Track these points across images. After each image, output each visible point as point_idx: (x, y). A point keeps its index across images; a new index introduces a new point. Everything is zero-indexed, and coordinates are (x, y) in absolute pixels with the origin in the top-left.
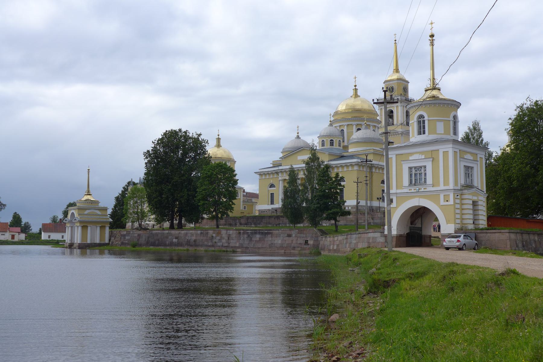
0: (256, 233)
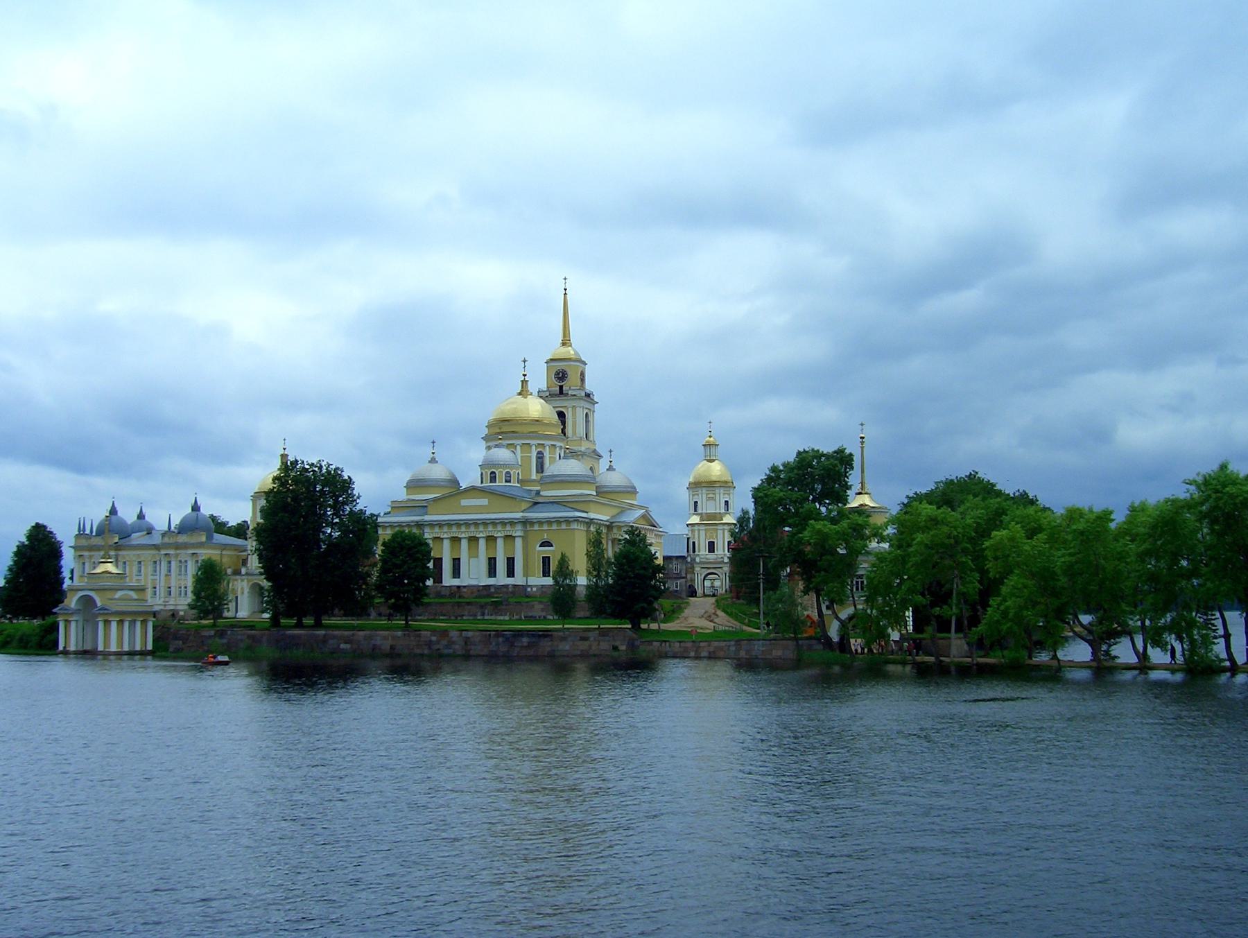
0: (522, 636)
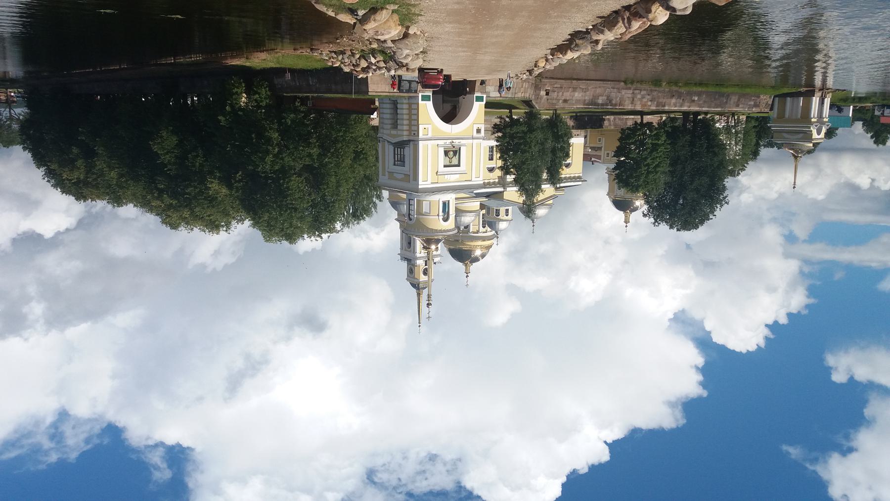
0: (602, 105)
